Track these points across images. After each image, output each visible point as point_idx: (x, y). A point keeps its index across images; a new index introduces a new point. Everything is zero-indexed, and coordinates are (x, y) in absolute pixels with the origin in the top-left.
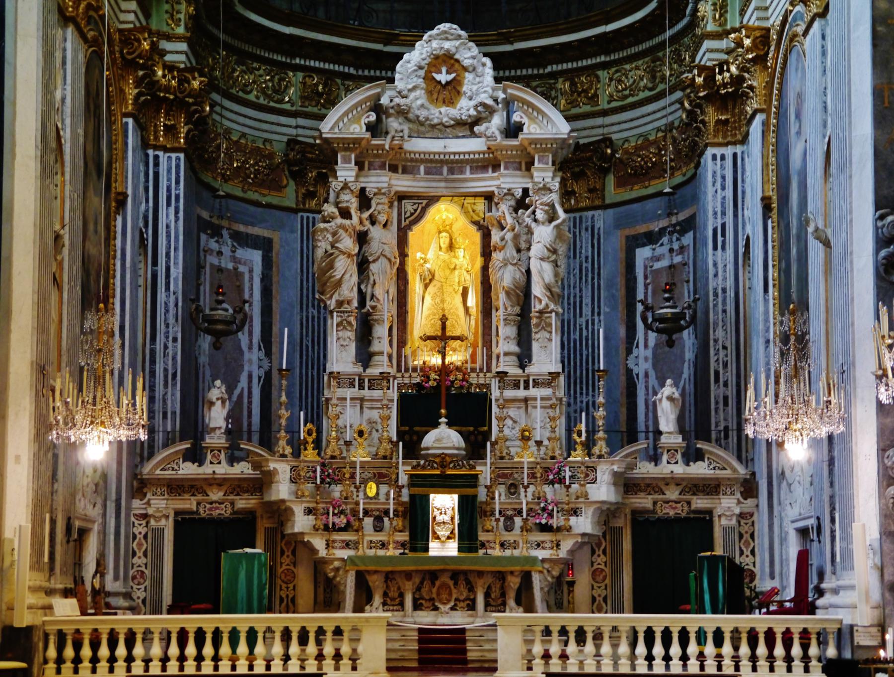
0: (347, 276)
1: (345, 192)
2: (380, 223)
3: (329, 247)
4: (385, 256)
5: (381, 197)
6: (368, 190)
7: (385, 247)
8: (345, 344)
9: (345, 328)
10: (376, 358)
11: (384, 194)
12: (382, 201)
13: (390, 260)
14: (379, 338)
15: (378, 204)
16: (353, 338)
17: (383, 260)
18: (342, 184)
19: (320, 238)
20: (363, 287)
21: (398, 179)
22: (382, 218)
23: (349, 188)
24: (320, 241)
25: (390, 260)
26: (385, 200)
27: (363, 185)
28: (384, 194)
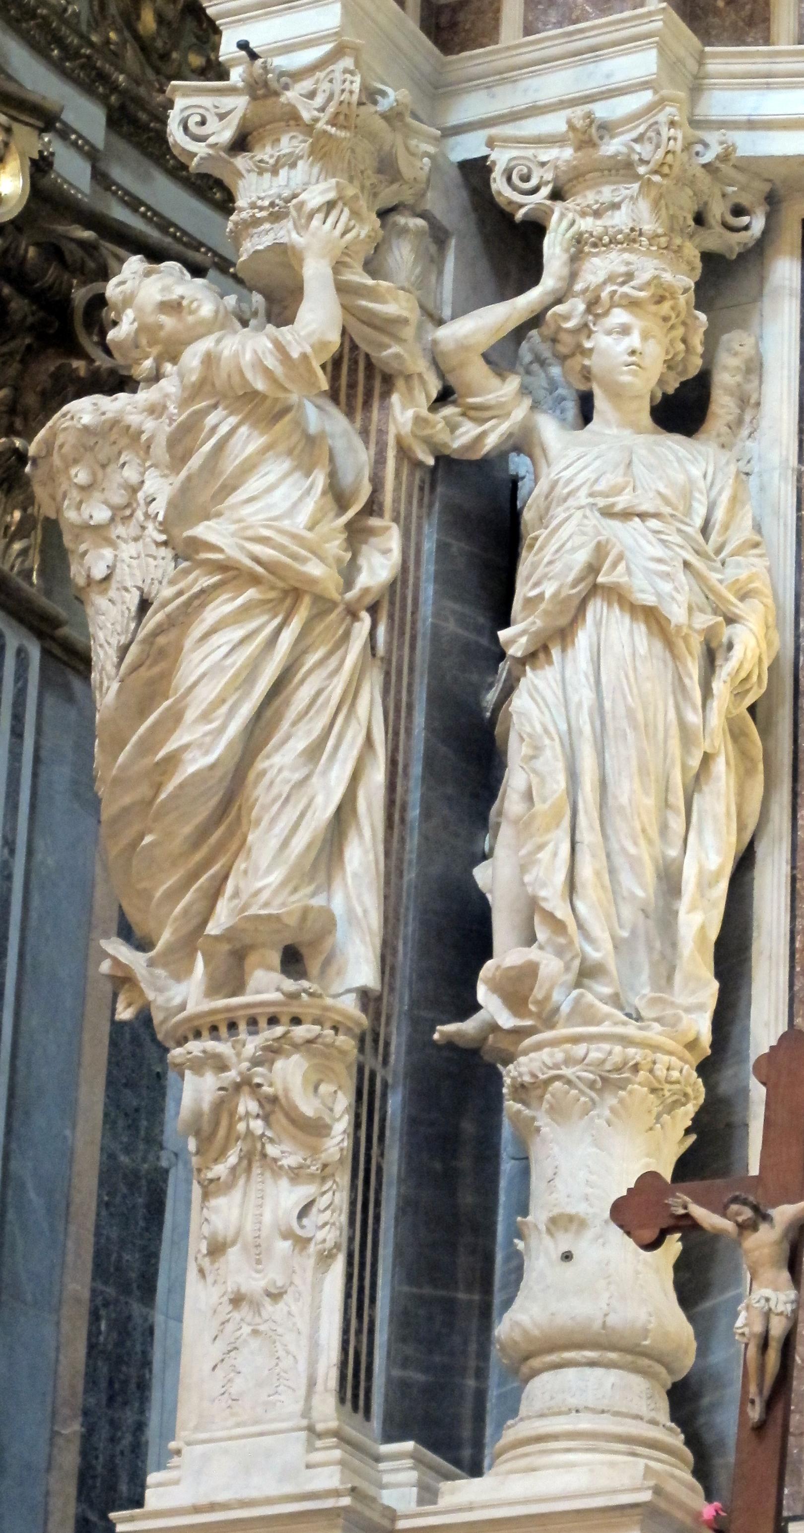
0: (280, 761)
1: (266, 153)
2: (617, 394)
3: (163, 563)
4: (617, 595)
5: (607, 193)
6: (501, 158)
7: (628, 536)
8: (254, 1283)
9: (255, 1157)
10: (542, 1389)
11: (623, 169)
12: (620, 220)
13: (651, 617)
14: (561, 1222)
15: (580, 250)
16: (330, 1223)
17: (608, 633)
18: (239, 104)
19: (101, 515)
20: (481, 874)
21: (766, 80)
22: (631, 352)
23: (292, 118)
24: (99, 533)
25: (651, 617)
26: (632, 210)
27: (470, 147)
28: (623, 169)
